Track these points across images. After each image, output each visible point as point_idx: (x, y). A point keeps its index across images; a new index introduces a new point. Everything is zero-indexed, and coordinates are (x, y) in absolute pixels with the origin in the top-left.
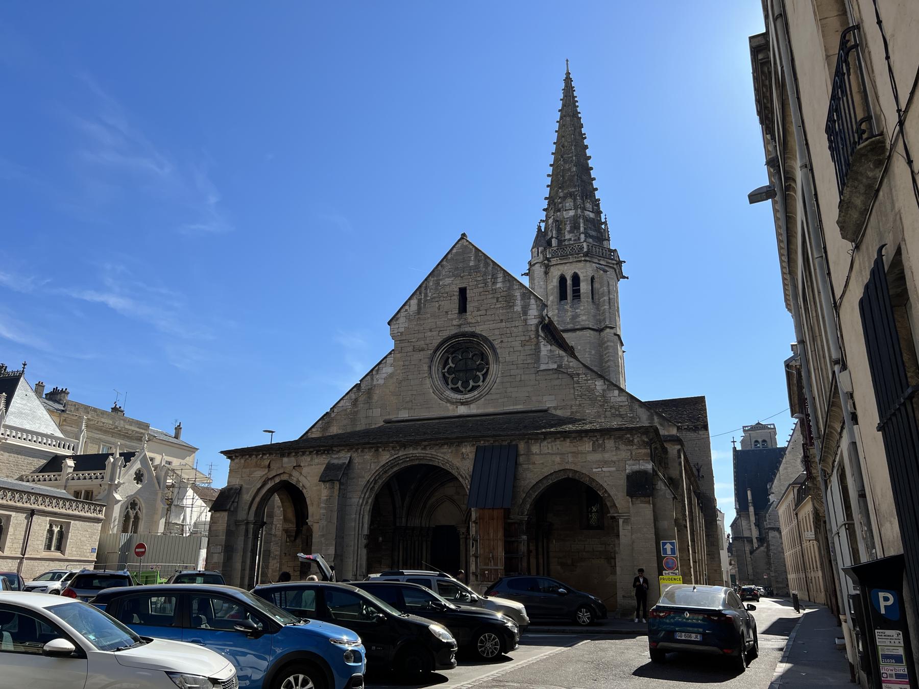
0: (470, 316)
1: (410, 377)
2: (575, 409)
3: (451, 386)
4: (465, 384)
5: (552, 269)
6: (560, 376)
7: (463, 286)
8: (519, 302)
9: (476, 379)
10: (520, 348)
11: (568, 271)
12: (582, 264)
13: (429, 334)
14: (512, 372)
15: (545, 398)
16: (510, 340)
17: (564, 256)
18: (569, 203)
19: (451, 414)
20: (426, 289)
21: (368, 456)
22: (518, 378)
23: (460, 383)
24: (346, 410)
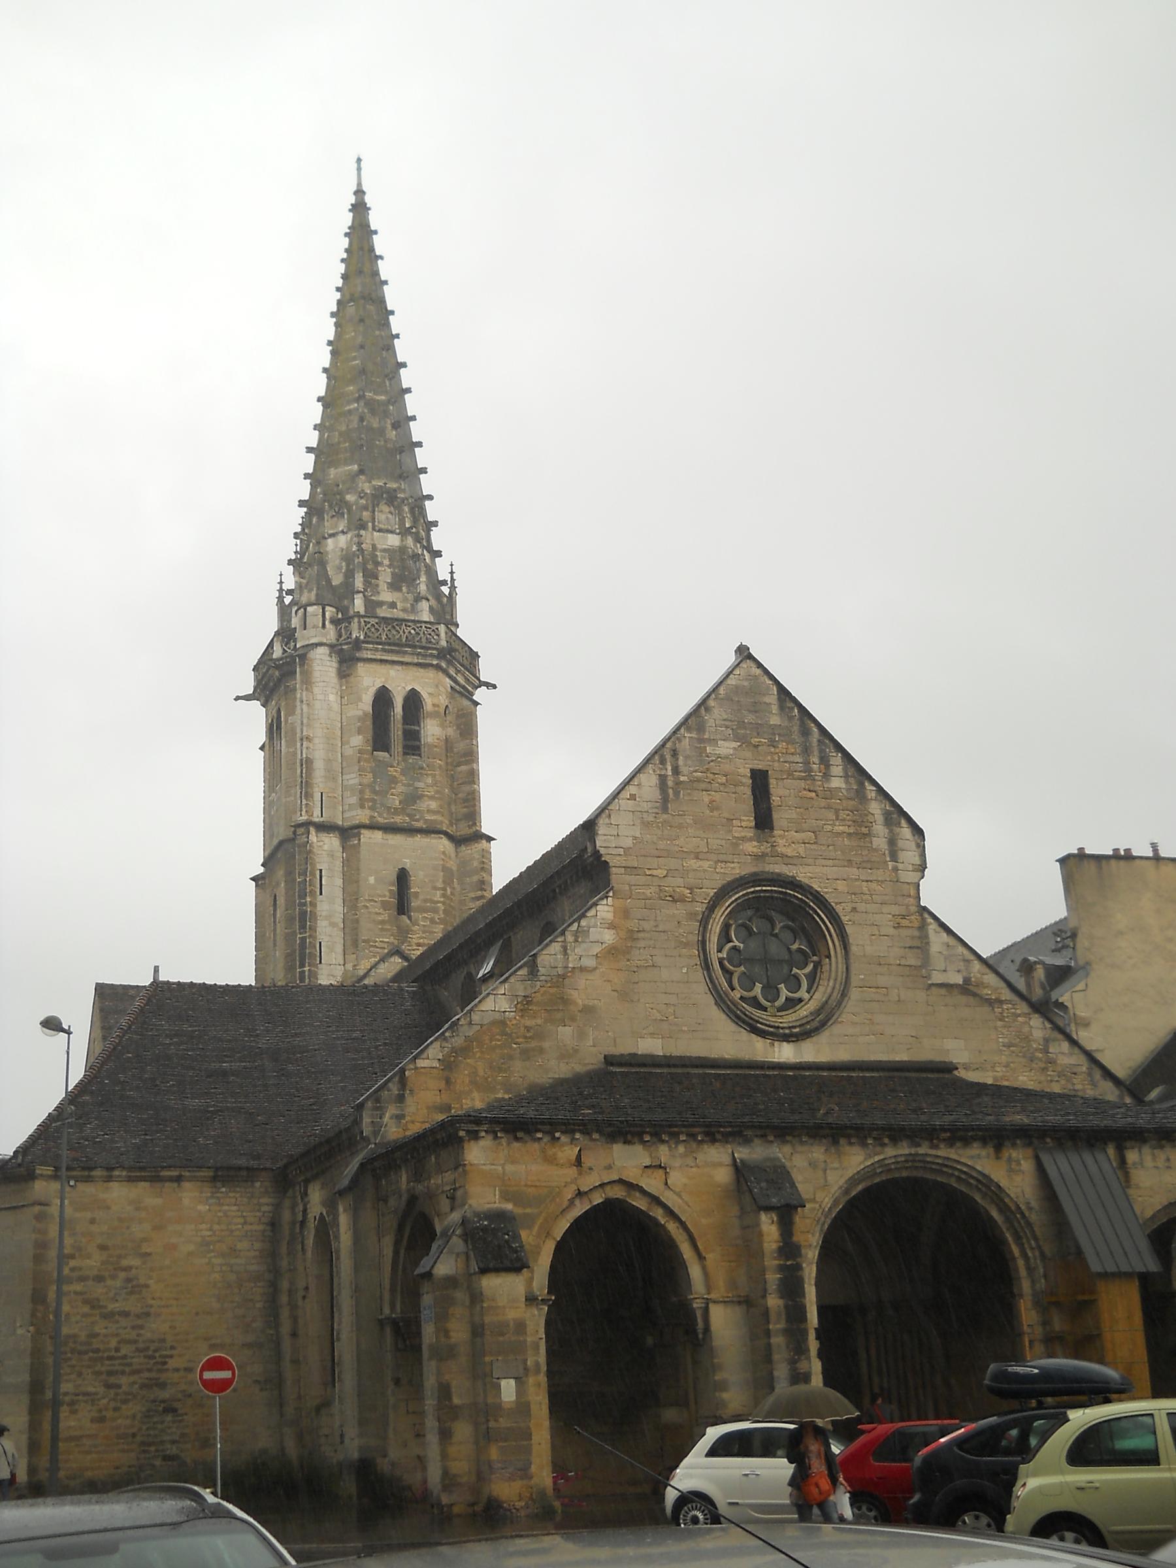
0: (786, 839)
1: (659, 960)
2: (1000, 1071)
4: (771, 990)
5: (361, 668)
7: (760, 766)
8: (880, 829)
10: (891, 931)
11: (400, 681)
12: (431, 674)
13: (692, 863)
14: (882, 980)
16: (871, 907)
17: (396, 646)
18: (384, 515)
20: (675, 754)
21: (818, 1152)
23: (758, 987)
24: (503, 1023)
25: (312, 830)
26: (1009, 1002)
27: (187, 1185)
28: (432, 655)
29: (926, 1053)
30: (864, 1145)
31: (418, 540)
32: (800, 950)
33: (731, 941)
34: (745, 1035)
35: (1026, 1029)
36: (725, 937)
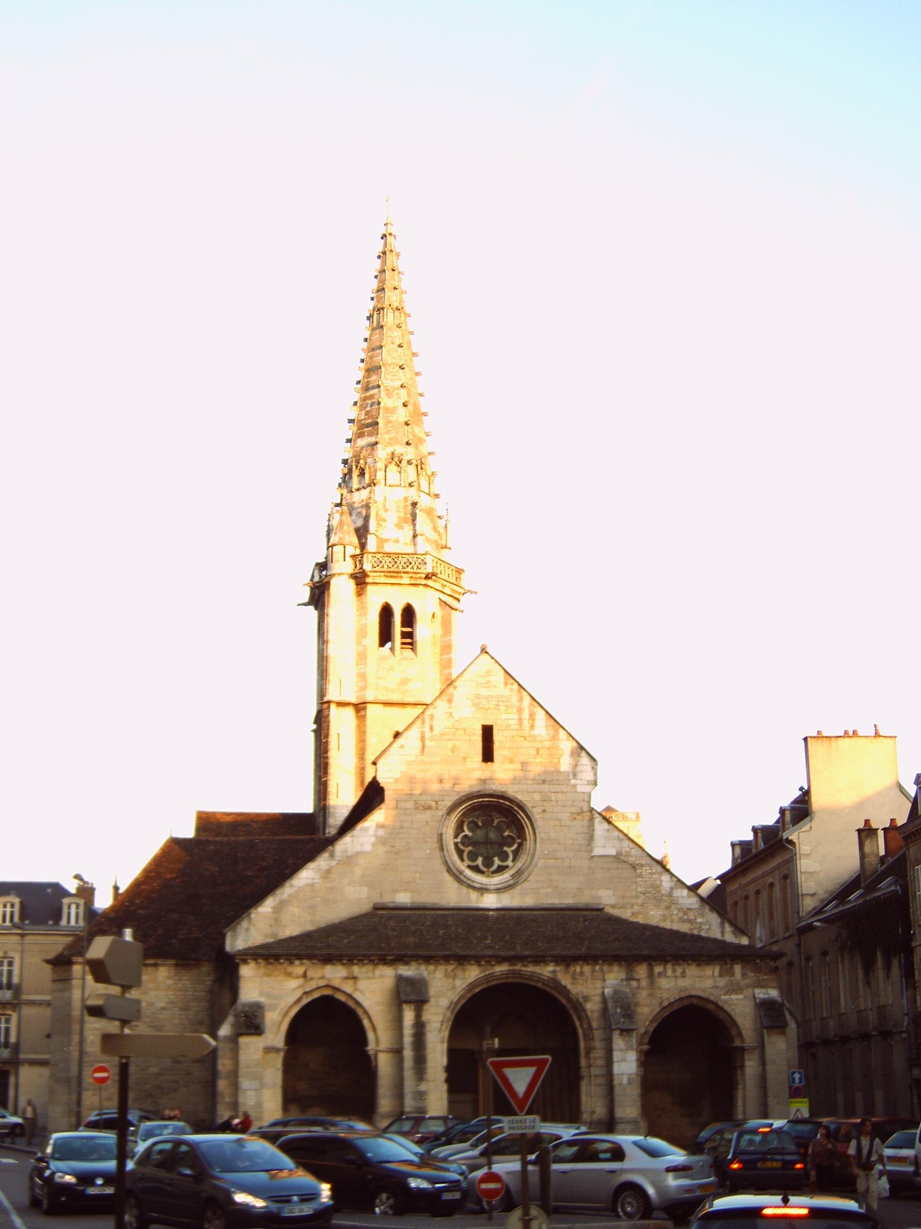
2: (636, 908)
3: (467, 862)
4: (488, 863)
6: (621, 866)
9: (504, 857)
22: (567, 864)
24: (312, 885)
25: (333, 706)
26: (649, 865)
27: (161, 969)
28: (420, 578)
29: (585, 898)
30: (480, 965)
31: (419, 490)
32: (509, 836)
33: (463, 831)
34: (464, 890)
35: (658, 882)
36: (459, 828)
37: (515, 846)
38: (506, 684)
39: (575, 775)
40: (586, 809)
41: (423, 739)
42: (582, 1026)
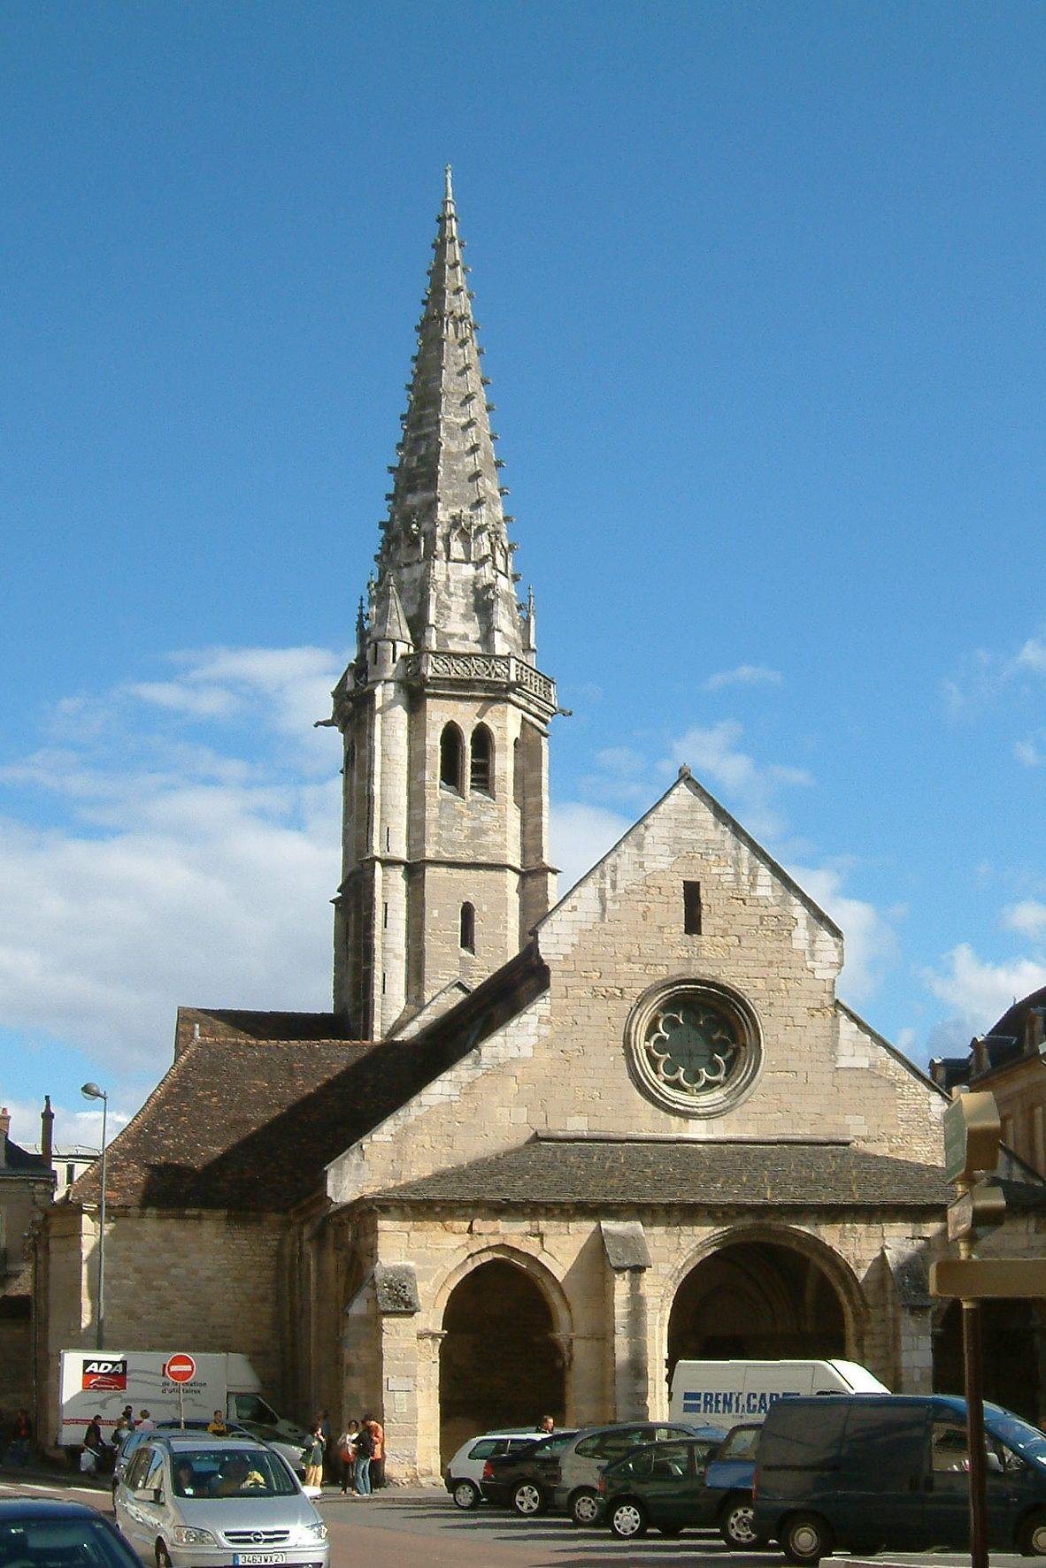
11: (466, 716)
13: (625, 967)
15: (849, 1120)
19: (674, 1135)
20: (615, 869)
25: (378, 865)
31: (494, 567)
37: (730, 1053)
38: (716, 826)
39: (812, 955)
40: (828, 1002)
41: (602, 899)
42: (851, 1301)
